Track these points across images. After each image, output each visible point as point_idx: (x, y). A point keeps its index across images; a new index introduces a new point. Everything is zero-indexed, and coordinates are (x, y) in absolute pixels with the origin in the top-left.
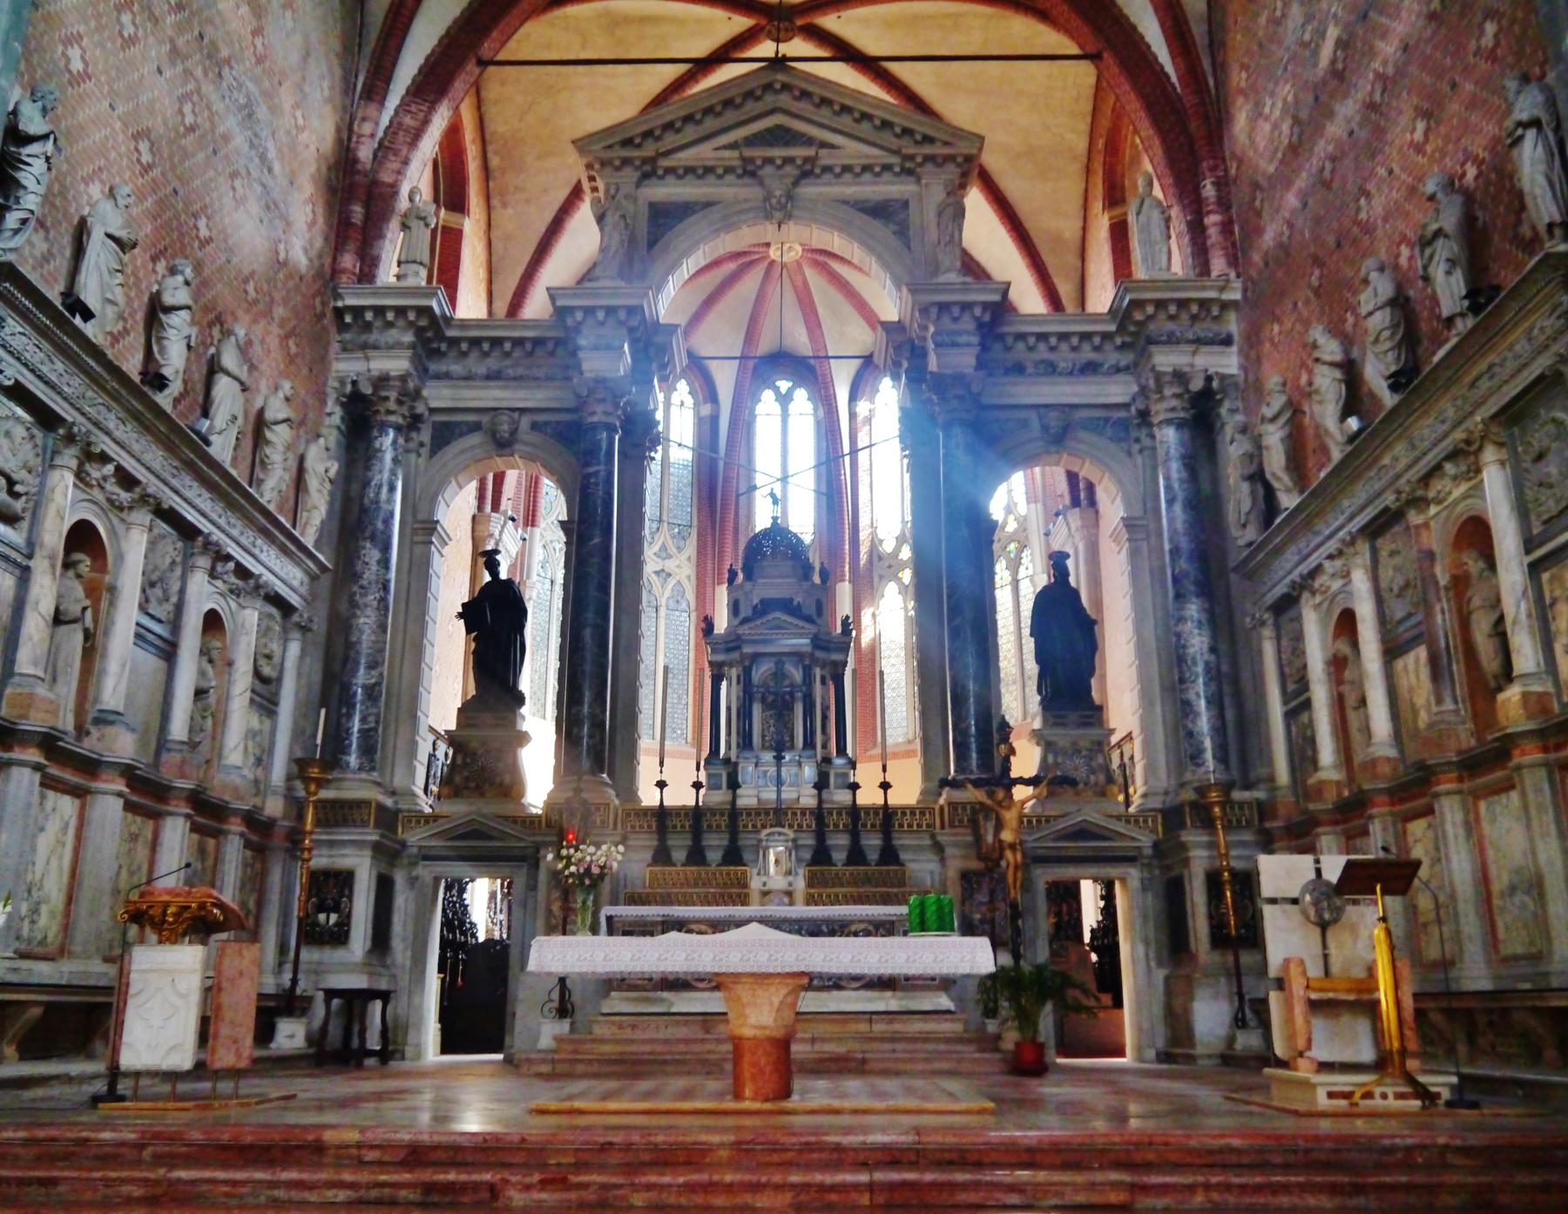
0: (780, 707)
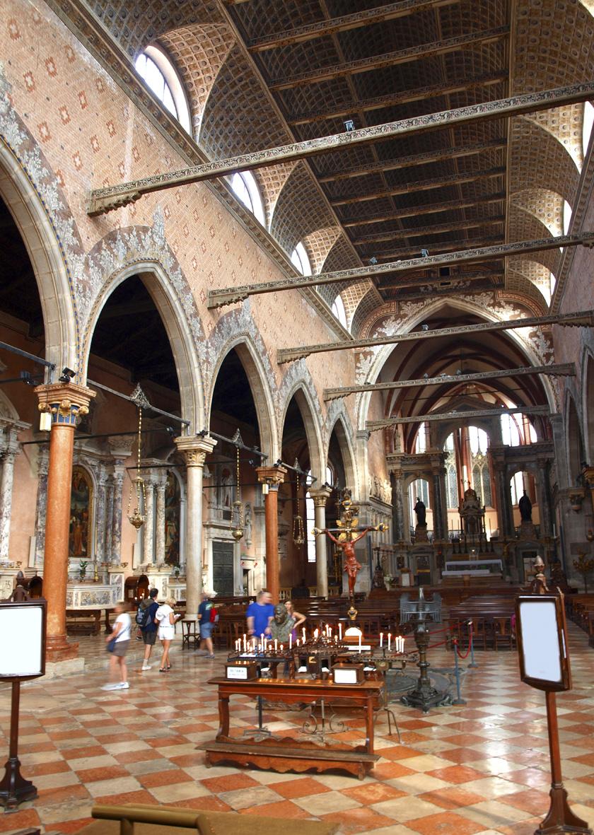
0: (473, 525)
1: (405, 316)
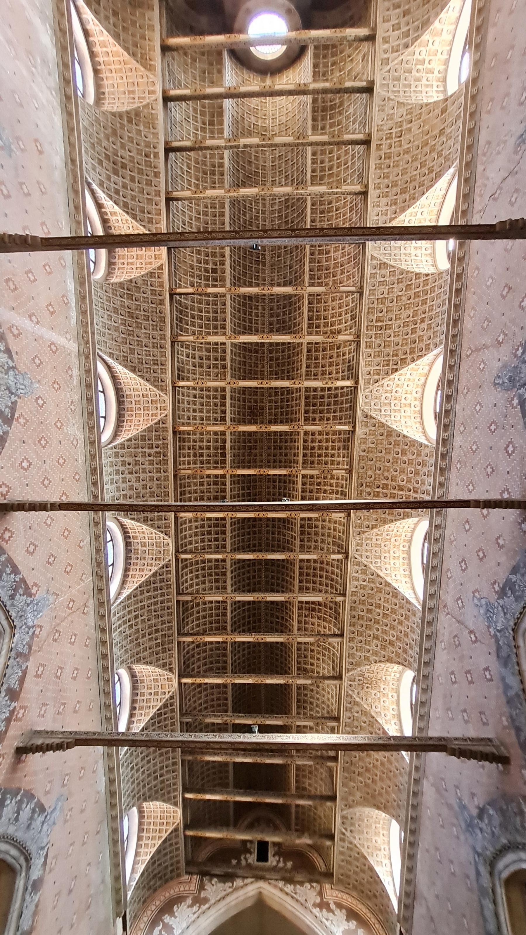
1: (206, 900)
